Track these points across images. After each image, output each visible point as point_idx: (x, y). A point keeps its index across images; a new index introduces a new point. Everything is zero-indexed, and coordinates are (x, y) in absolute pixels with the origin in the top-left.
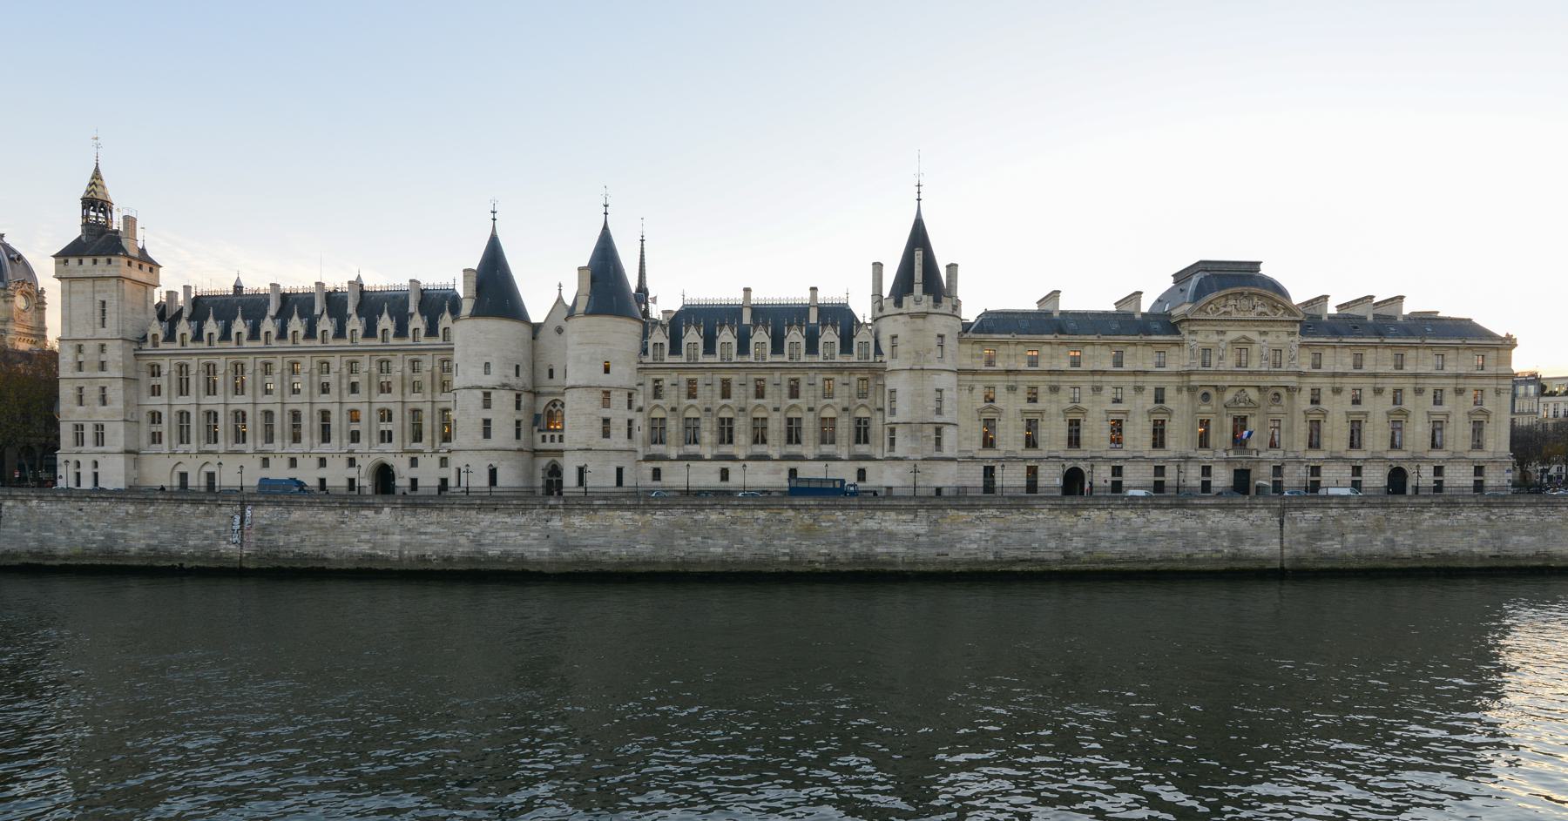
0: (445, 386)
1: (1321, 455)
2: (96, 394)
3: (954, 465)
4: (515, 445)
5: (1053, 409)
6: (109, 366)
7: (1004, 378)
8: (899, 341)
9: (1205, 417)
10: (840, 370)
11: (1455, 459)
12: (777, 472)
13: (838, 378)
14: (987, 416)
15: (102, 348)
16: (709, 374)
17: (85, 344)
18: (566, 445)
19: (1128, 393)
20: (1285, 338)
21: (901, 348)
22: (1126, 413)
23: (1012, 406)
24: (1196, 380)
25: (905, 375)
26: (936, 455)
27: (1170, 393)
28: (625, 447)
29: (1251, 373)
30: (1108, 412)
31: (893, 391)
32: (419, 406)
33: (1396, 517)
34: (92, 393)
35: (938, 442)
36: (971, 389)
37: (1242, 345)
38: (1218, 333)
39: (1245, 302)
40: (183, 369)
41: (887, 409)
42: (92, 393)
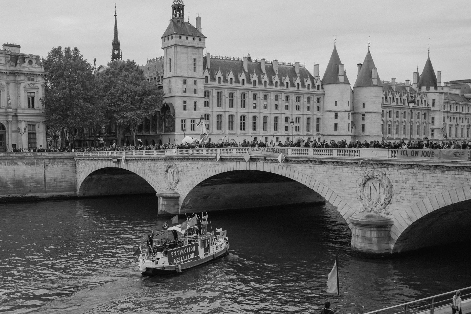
0: (318, 109)
2: (192, 106)
5: (454, 125)
6: (198, 91)
7: (446, 114)
10: (421, 110)
13: (421, 112)
15: (195, 82)
16: (395, 109)
17: (188, 80)
18: (367, 133)
21: (436, 103)
22: (464, 126)
30: (461, 126)
31: (433, 118)
32: (310, 116)
34: (190, 105)
40: (219, 94)
41: (431, 123)
42: (190, 105)
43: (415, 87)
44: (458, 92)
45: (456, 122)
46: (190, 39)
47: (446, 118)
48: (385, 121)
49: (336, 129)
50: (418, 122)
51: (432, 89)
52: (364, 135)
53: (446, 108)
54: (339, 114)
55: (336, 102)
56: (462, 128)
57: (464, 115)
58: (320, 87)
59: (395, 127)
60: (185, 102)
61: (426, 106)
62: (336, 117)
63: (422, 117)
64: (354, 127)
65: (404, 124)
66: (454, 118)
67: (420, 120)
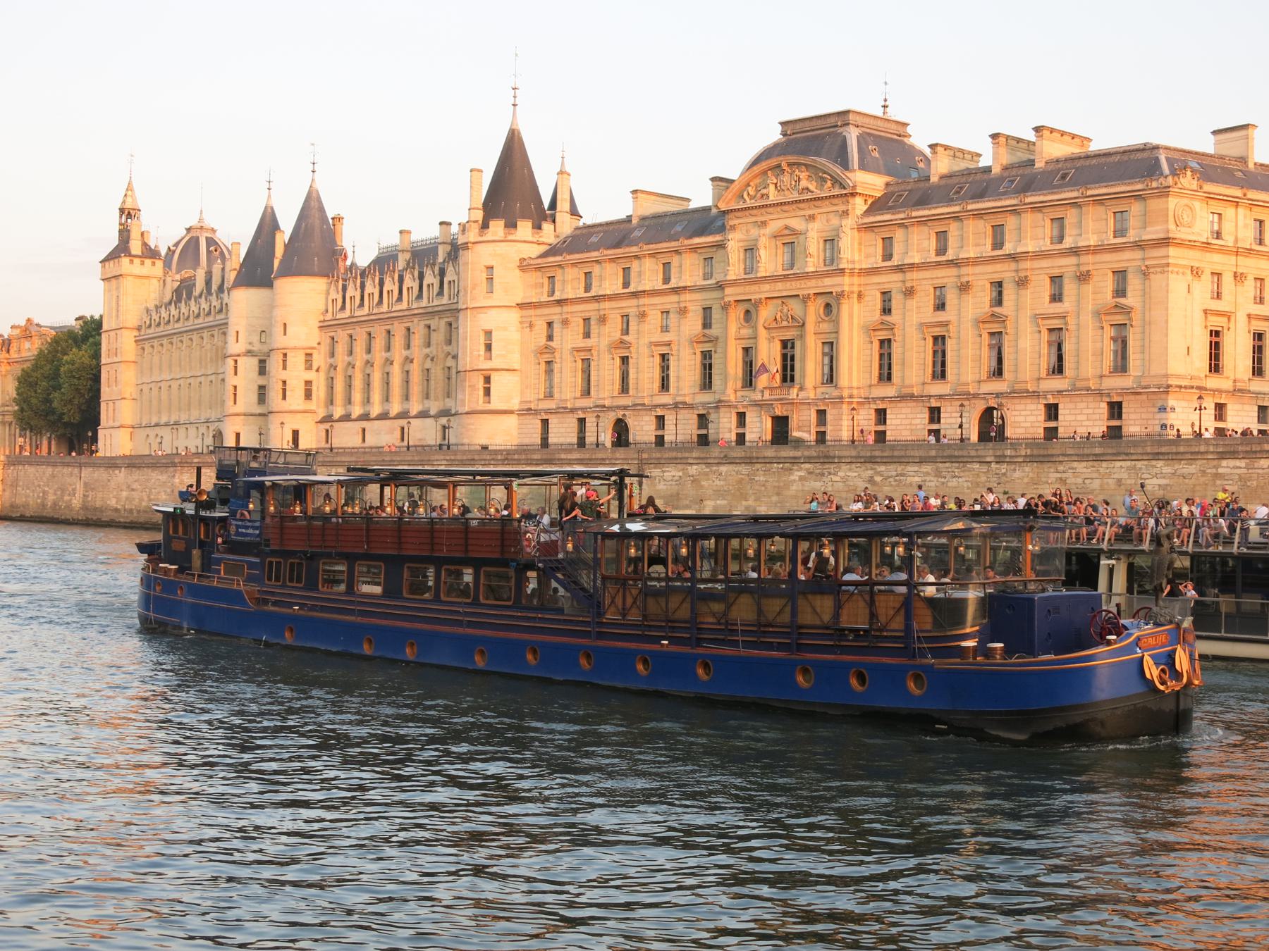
1: (889, 391)
3: (512, 421)
4: (259, 410)
11: (1079, 391)
12: (391, 431)
13: (433, 323)
20: (835, 221)
23: (568, 339)
26: (481, 405)
28: (301, 408)
29: (765, 280)
30: (657, 344)
33: (760, 478)
35: (487, 392)
36: (531, 326)
37: (790, 241)
39: (786, 178)
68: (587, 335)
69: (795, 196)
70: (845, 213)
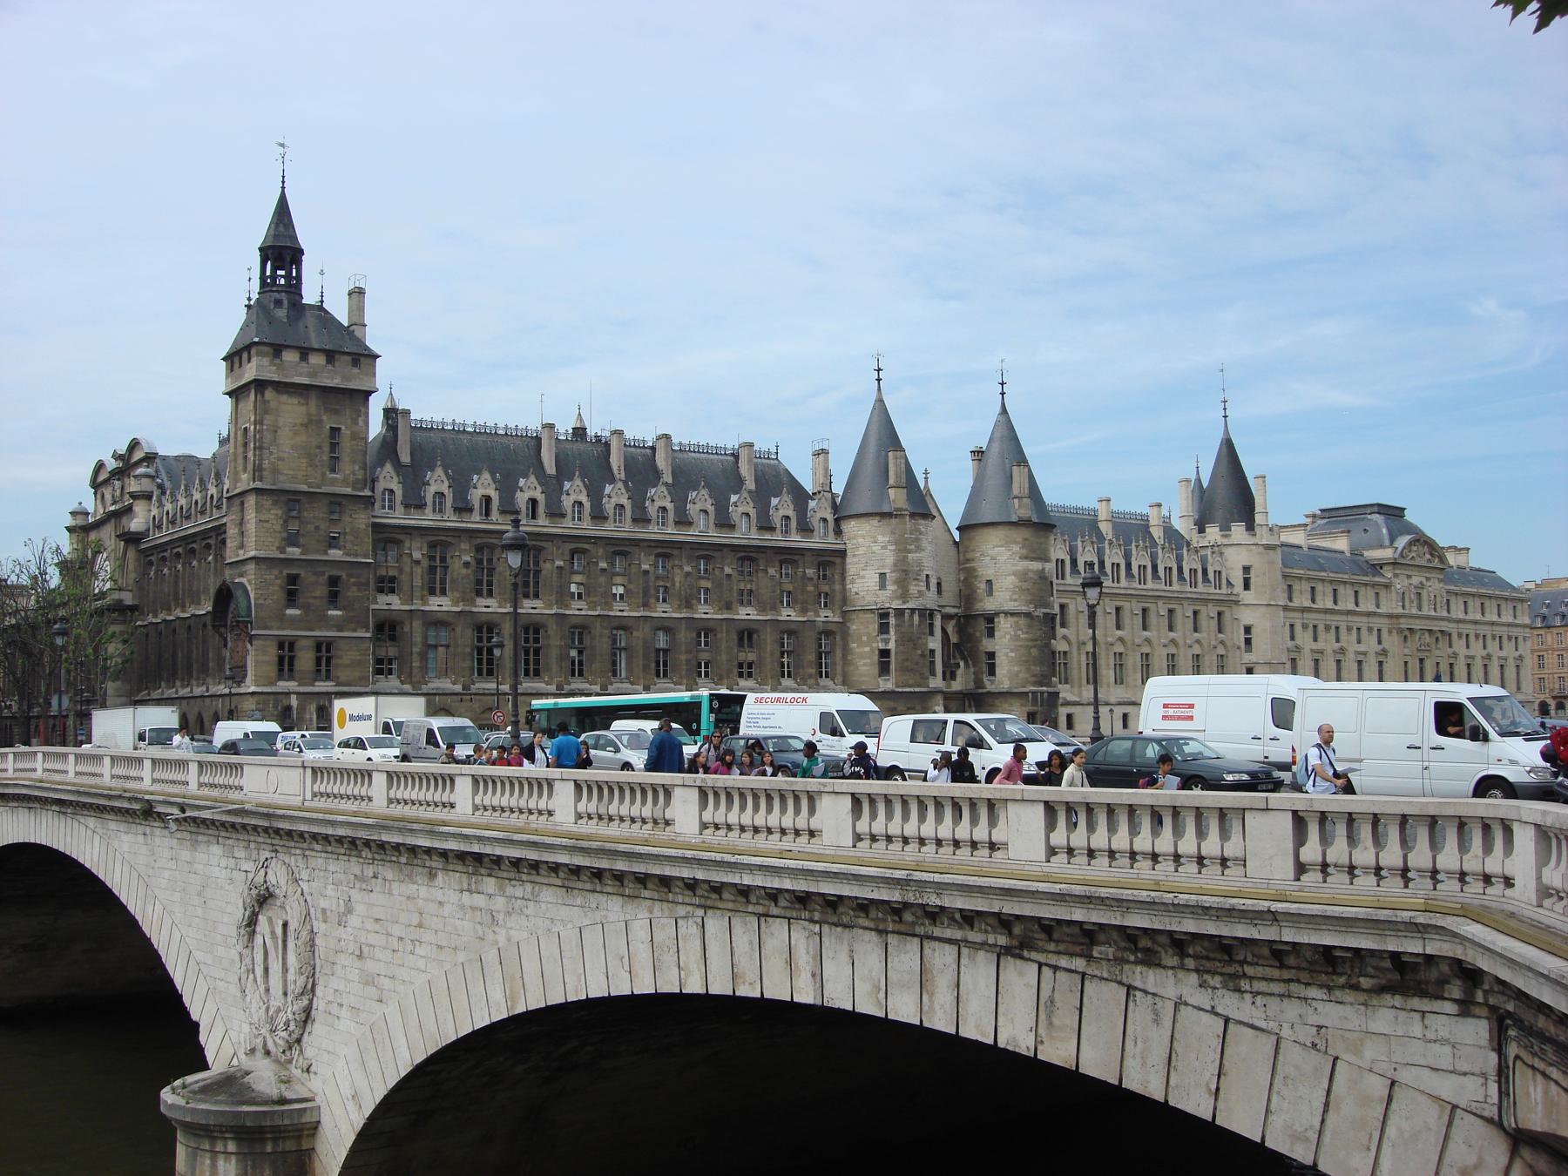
5: (1329, 651)
7: (1298, 615)
8: (1252, 574)
9: (1407, 659)
13: (1203, 609)
14: (1293, 655)
19: (1364, 632)
20: (1438, 585)
22: (1364, 654)
24: (1404, 624)
25: (1263, 609)
27: (1385, 634)
31: (1248, 630)
38: (1409, 577)
41: (1243, 645)
43: (1183, 526)
44: (1341, 544)
45: (1338, 640)
46: (317, 360)
47: (1298, 628)
48: (1074, 641)
49: (884, 669)
50: (1198, 641)
51: (1238, 531)
52: (990, 687)
53: (1296, 595)
54: (892, 621)
55: (883, 576)
56: (1360, 662)
57: (1365, 619)
58: (831, 524)
59: (1112, 662)
60: (293, 579)
61: (1224, 591)
62: (884, 628)
63: (1209, 625)
64: (962, 664)
65: (1146, 650)
66: (1327, 628)
67: (1205, 635)
68: (1315, 639)
69: (1423, 563)
70: (1440, 581)
